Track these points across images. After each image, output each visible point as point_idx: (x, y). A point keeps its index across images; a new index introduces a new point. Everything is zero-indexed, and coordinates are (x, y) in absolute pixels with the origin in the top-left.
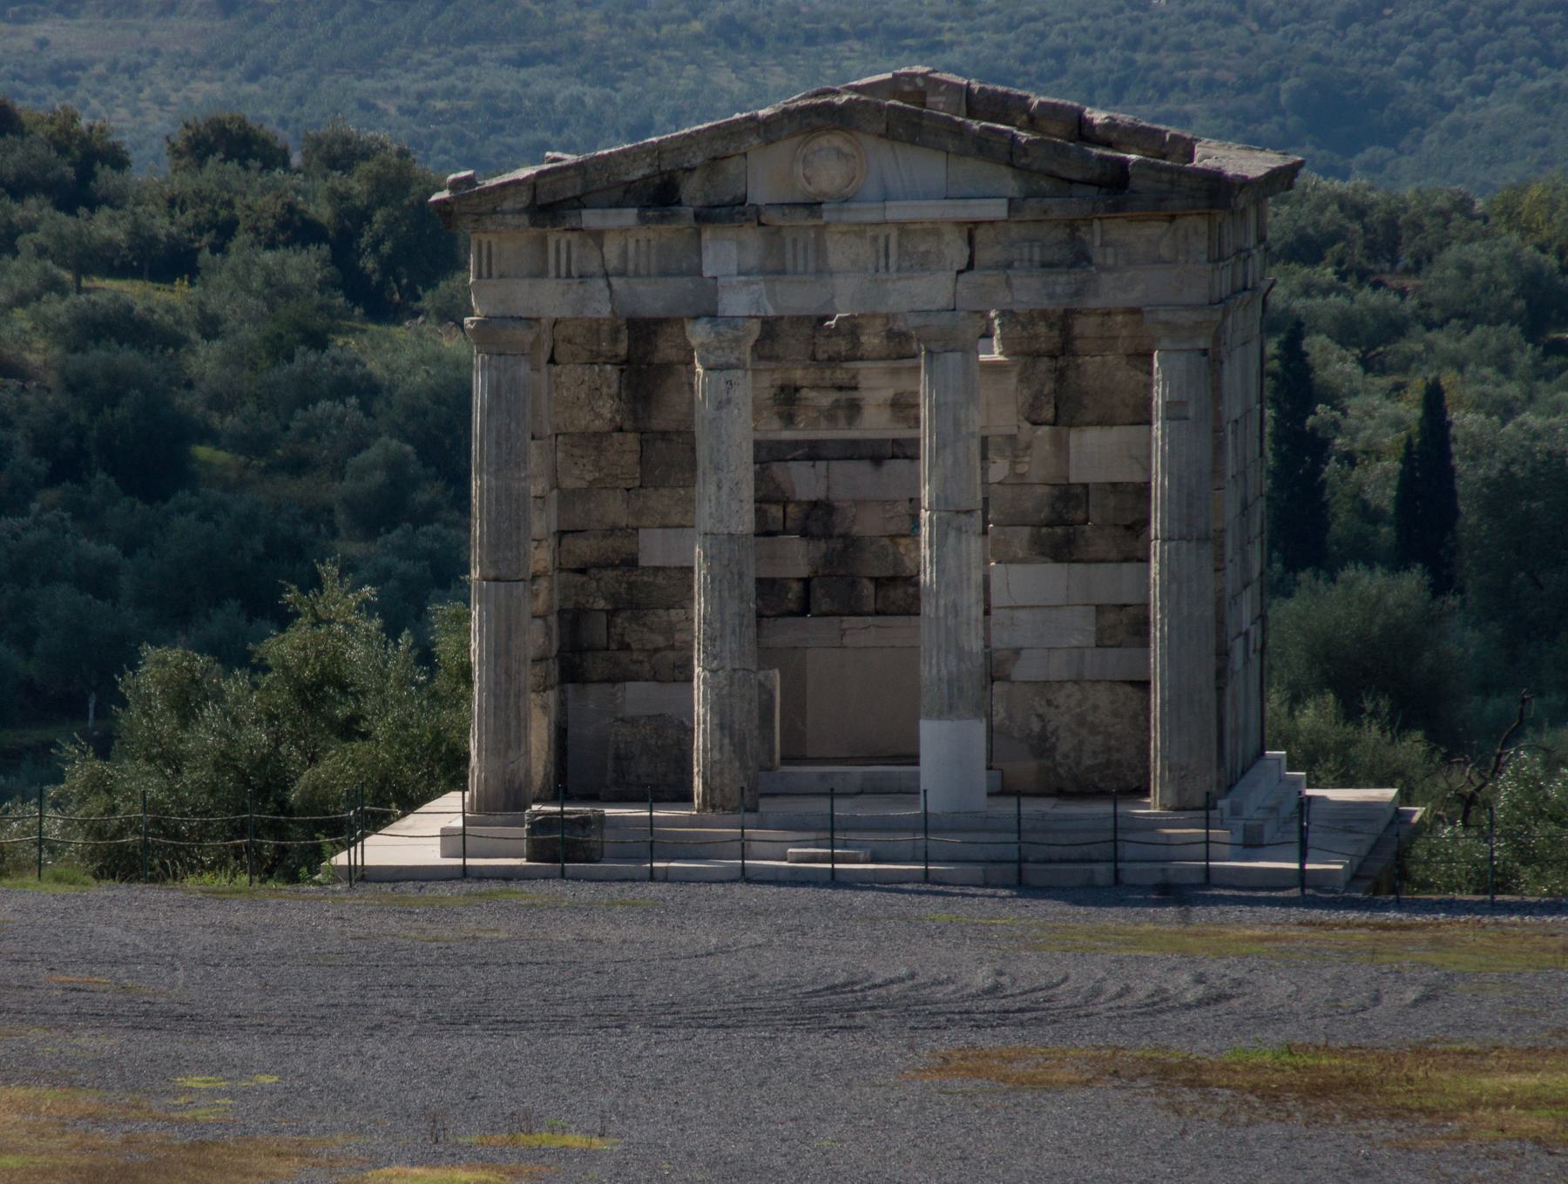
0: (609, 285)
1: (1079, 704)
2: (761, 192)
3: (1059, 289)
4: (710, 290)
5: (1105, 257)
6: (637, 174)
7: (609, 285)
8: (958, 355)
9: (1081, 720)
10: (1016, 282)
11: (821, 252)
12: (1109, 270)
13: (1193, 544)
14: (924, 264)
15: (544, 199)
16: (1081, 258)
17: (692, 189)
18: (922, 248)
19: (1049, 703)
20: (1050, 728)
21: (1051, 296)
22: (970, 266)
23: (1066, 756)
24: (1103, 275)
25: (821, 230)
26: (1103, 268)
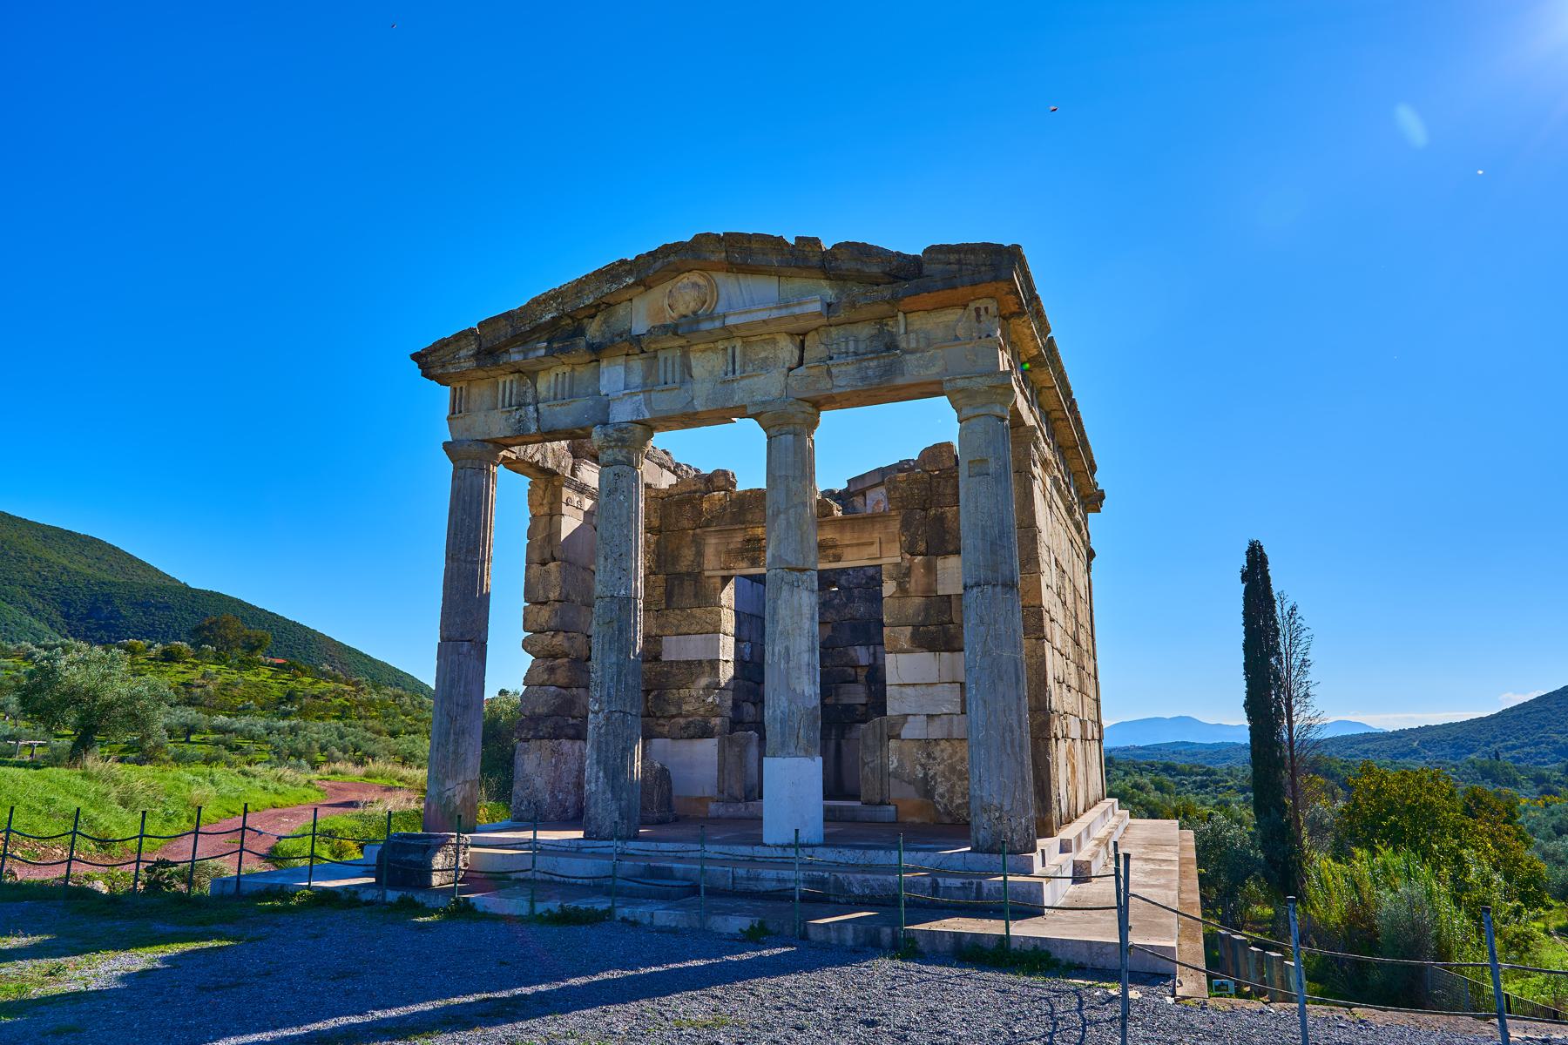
0: (537, 410)
1: (951, 757)
2: (640, 326)
3: (870, 372)
4: (605, 406)
5: (908, 342)
6: (549, 317)
7: (537, 410)
8: (791, 437)
9: (952, 769)
10: (834, 370)
11: (687, 368)
12: (912, 352)
13: (999, 589)
14: (765, 366)
15: (486, 345)
16: (891, 346)
17: (594, 330)
18: (763, 355)
19: (929, 756)
20: (931, 773)
21: (863, 379)
22: (801, 363)
23: (942, 796)
24: (908, 357)
25: (685, 351)
26: (905, 352)
